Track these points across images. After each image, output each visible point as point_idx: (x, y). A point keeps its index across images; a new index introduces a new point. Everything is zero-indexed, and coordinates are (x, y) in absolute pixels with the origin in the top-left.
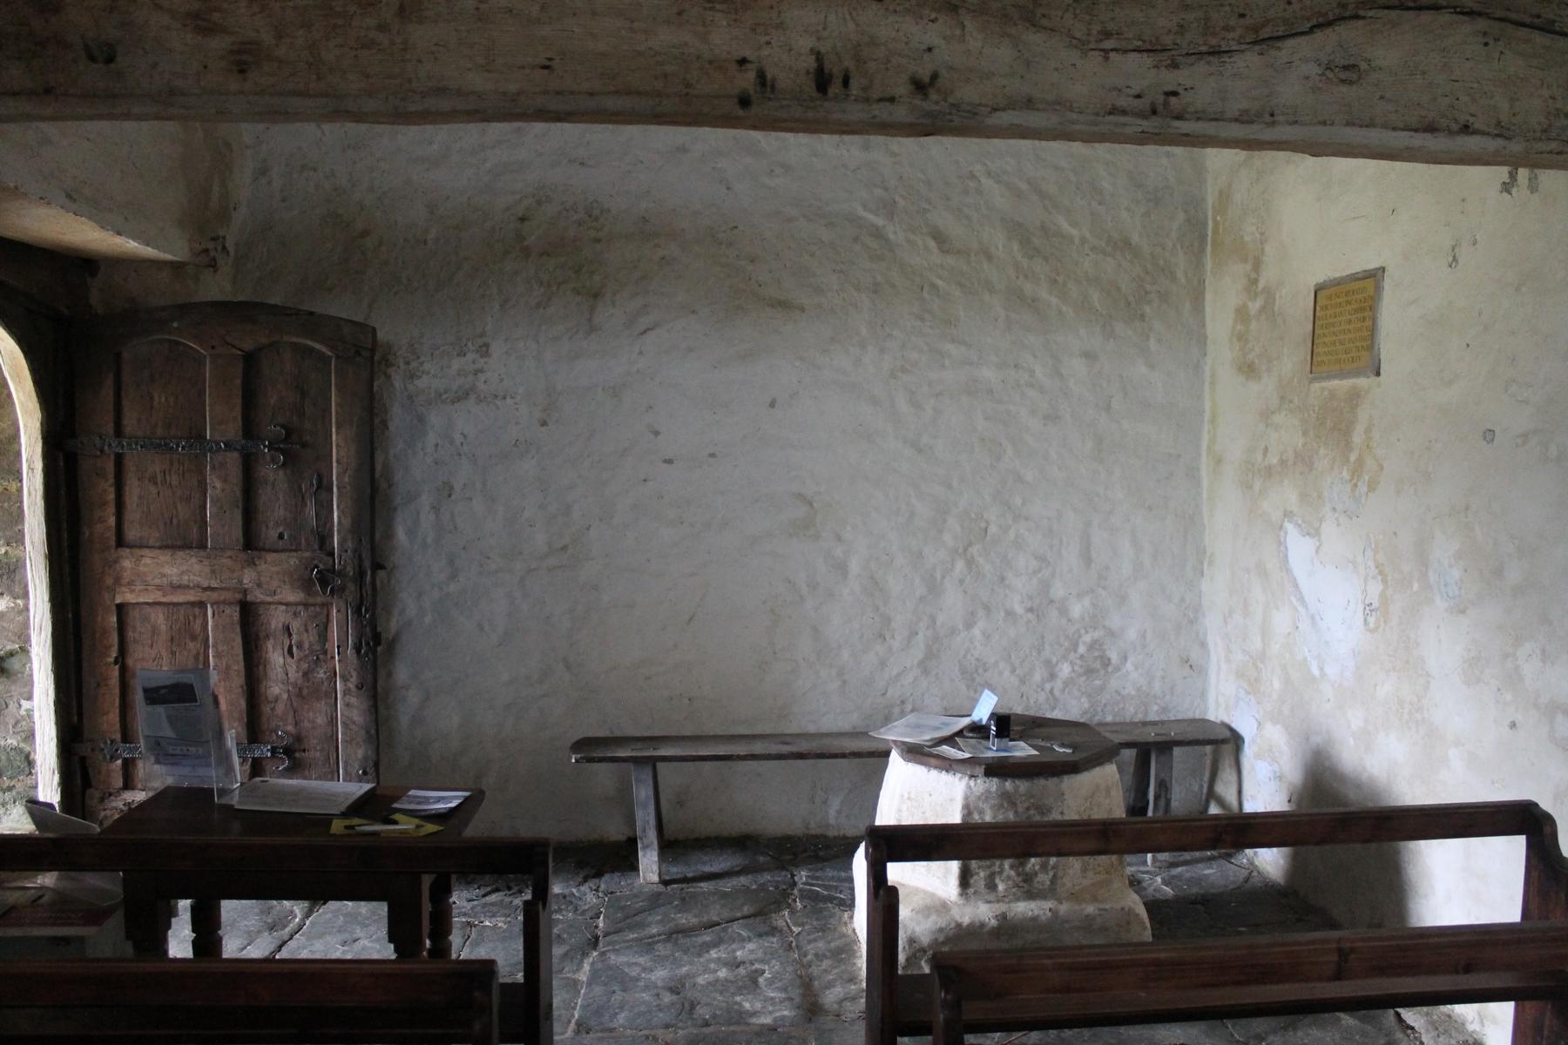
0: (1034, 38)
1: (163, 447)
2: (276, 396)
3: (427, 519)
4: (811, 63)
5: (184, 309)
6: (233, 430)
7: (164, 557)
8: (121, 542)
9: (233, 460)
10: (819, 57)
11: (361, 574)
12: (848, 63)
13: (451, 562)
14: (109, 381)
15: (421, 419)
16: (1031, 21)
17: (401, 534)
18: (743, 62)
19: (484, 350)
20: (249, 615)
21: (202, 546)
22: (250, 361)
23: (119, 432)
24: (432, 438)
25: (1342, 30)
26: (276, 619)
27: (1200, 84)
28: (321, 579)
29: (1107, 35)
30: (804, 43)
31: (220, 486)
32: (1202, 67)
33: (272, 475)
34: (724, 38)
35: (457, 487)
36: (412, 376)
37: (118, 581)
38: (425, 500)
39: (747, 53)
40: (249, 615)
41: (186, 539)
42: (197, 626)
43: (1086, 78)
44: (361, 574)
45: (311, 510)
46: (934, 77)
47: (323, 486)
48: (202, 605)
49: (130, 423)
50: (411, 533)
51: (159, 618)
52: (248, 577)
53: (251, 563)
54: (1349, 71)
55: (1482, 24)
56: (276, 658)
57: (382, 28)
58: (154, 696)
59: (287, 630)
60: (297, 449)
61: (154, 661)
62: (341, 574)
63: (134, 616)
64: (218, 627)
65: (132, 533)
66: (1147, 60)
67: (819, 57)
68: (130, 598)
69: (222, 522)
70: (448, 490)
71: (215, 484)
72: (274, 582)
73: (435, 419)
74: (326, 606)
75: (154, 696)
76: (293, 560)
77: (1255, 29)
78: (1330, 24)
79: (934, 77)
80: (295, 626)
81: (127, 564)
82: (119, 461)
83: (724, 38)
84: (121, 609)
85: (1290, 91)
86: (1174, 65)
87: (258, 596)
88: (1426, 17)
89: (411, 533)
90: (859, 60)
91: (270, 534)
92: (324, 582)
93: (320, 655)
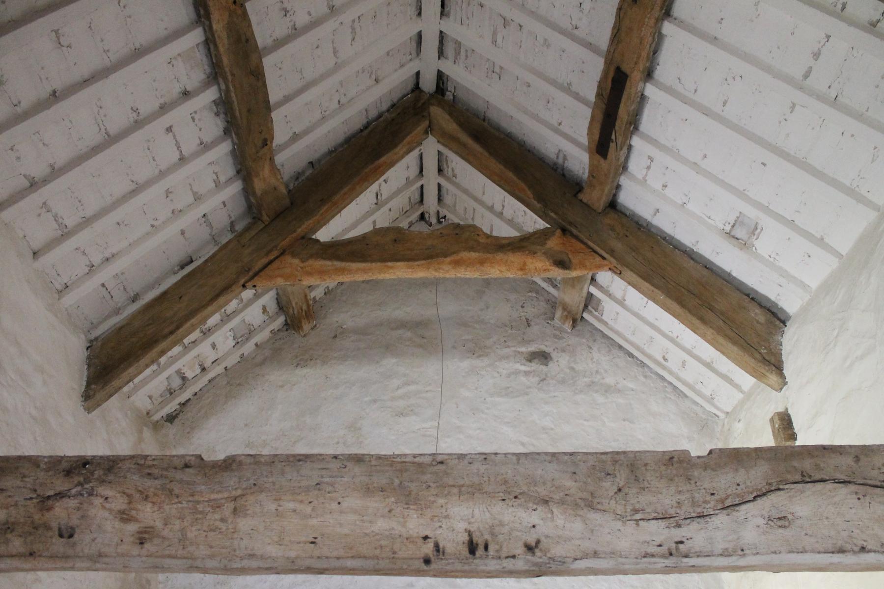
0: (592, 515)
4: (466, 538)
10: (470, 534)
12: (487, 536)
16: (591, 506)
18: (426, 538)
25: (773, 498)
27: (696, 535)
29: (636, 511)
30: (461, 526)
32: (694, 525)
34: (415, 524)
39: (427, 533)
43: (627, 537)
46: (538, 542)
54: (782, 521)
55: (852, 488)
57: (222, 520)
66: (662, 524)
67: (470, 534)
77: (722, 501)
78: (764, 494)
79: (538, 542)
83: (415, 524)
85: (749, 536)
86: (679, 526)
88: (819, 486)
90: (493, 534)
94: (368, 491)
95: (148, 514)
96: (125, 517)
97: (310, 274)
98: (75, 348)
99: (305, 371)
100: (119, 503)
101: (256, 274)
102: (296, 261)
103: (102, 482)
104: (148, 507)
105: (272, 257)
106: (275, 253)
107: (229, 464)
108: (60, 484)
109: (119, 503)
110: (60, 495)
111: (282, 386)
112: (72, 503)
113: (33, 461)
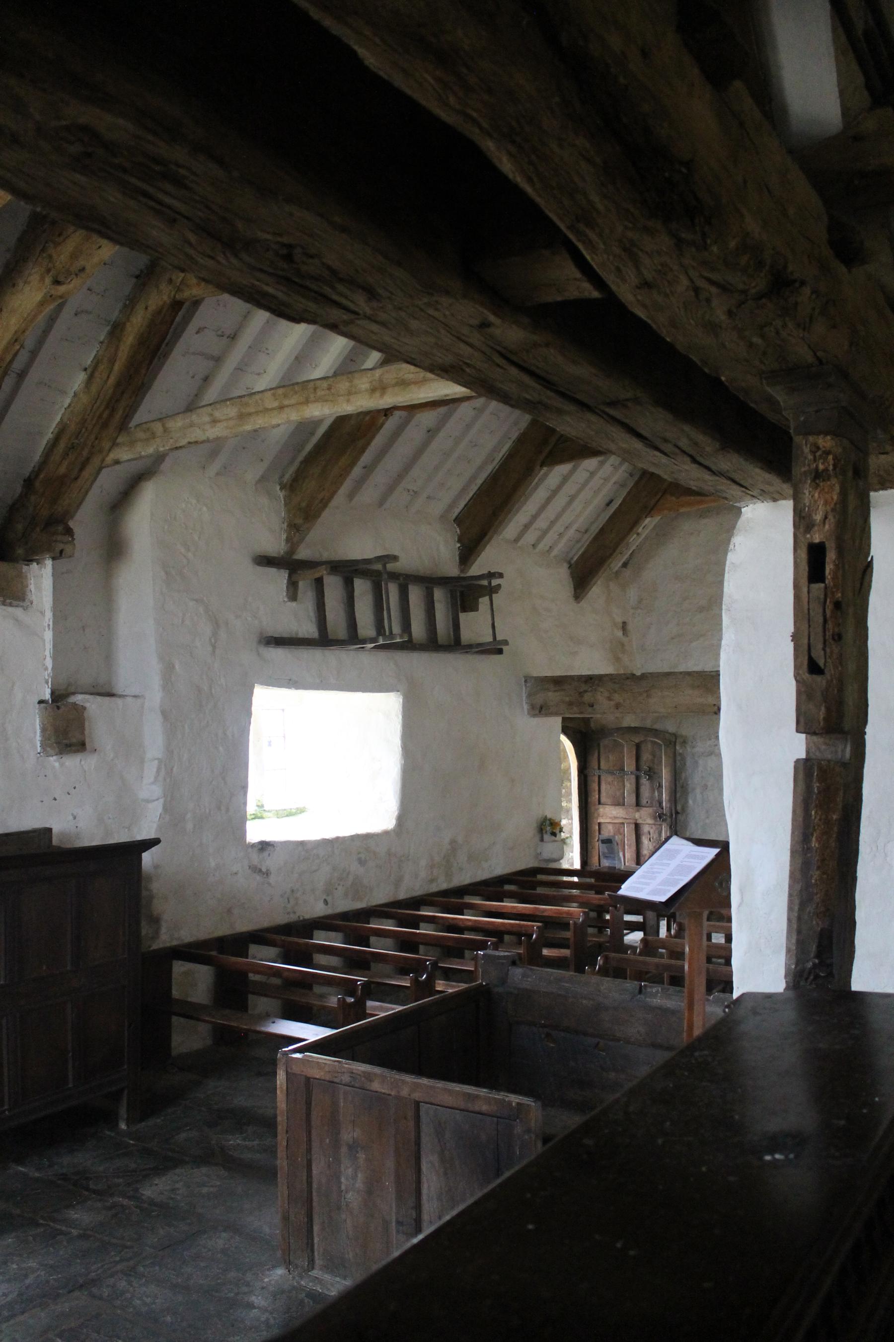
1: (612, 773)
2: (646, 757)
3: (699, 796)
5: (619, 729)
6: (633, 767)
7: (612, 808)
8: (599, 803)
9: (633, 778)
11: (672, 815)
13: (707, 812)
14: (596, 755)
15: (696, 762)
17: (690, 802)
20: (637, 827)
21: (624, 805)
22: (638, 747)
23: (599, 768)
24: (700, 769)
26: (645, 829)
28: (660, 816)
31: (629, 785)
35: (709, 784)
36: (694, 747)
37: (599, 815)
38: (698, 791)
40: (637, 827)
42: (622, 830)
44: (672, 815)
45: (656, 794)
47: (660, 786)
48: (623, 823)
50: (694, 801)
51: (610, 827)
52: (637, 815)
53: (638, 811)
56: (645, 841)
58: (603, 842)
59: (649, 833)
60: (652, 774)
62: (666, 815)
63: (603, 826)
65: (603, 800)
69: (630, 798)
70: (705, 787)
72: (645, 817)
73: (701, 762)
74: (661, 825)
75: (603, 842)
76: (650, 810)
80: (652, 831)
81: (601, 810)
82: (599, 777)
84: (599, 824)
87: (640, 821)
91: (644, 801)
92: (660, 817)
94: (693, 687)
95: (617, 697)
96: (609, 699)
97: (682, 506)
98: (563, 573)
99: (705, 521)
100: (606, 694)
101: (652, 509)
102: (674, 498)
103: (598, 686)
104: (616, 695)
105: (658, 497)
106: (660, 494)
107: (644, 676)
108: (584, 687)
109: (606, 694)
110: (586, 691)
111: (692, 534)
112: (589, 694)
113: (571, 677)
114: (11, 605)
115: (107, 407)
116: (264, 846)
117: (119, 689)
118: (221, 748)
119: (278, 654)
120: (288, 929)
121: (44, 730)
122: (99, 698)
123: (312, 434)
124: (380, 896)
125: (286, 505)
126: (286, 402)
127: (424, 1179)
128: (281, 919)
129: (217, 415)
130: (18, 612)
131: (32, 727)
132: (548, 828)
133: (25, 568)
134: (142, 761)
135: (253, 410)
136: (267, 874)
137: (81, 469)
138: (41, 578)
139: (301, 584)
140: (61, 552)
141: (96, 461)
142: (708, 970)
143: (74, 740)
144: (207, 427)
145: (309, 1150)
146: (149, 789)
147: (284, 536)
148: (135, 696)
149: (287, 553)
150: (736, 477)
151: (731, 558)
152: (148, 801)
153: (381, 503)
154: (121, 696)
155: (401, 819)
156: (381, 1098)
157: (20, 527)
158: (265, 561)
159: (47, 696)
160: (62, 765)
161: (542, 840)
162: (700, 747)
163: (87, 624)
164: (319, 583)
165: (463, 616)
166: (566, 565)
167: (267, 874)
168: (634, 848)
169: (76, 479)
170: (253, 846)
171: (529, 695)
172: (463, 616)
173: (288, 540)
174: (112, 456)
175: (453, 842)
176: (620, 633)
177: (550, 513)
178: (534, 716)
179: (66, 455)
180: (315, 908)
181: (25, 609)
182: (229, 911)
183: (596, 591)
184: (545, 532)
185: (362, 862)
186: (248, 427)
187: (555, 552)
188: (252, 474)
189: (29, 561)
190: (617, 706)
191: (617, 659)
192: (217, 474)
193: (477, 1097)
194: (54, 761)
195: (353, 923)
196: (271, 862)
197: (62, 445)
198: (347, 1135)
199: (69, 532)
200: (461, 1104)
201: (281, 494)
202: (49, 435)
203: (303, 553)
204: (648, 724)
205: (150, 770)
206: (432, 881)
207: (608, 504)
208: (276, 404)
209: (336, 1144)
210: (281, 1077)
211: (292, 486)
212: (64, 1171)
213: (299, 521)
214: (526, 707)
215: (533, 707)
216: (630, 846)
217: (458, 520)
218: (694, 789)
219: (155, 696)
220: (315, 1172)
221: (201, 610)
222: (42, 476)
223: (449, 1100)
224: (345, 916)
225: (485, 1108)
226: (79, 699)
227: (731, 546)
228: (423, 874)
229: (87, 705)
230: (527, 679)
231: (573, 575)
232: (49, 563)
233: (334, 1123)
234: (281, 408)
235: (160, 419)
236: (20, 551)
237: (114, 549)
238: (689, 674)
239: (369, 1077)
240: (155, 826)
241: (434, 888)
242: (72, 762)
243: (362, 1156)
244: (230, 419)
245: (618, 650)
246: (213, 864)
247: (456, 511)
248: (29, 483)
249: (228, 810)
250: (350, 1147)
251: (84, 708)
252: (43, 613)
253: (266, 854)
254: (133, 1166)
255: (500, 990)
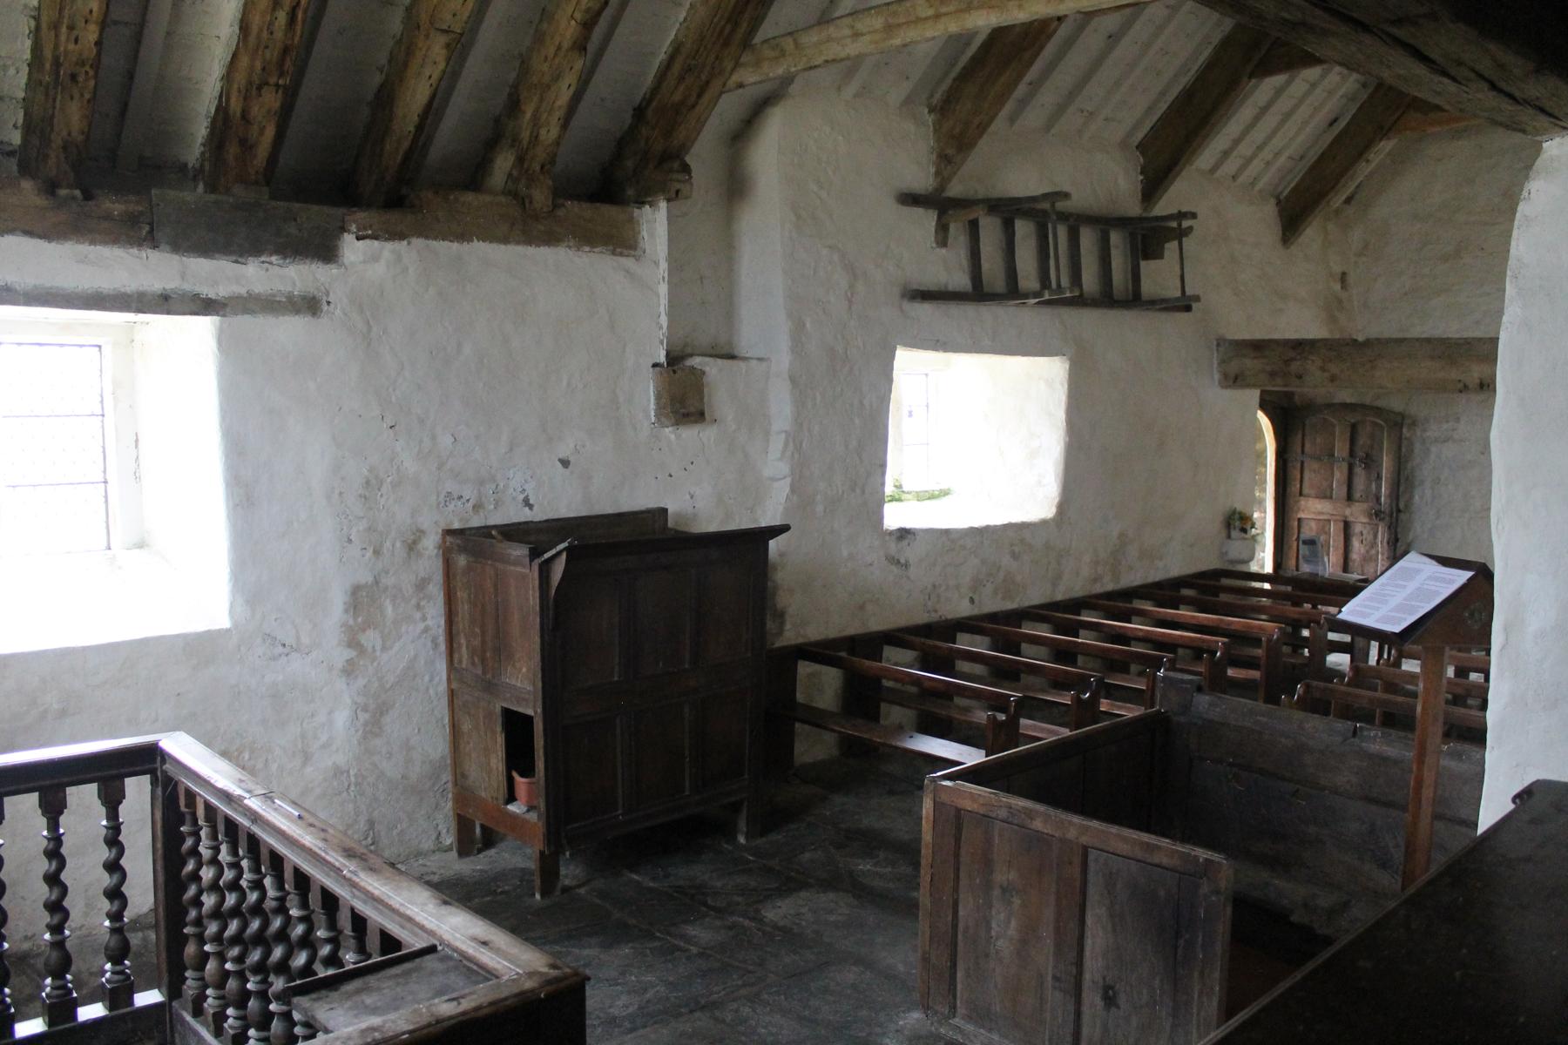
1: (1319, 459)
2: (1362, 440)
3: (1428, 492)
5: (1330, 406)
6: (1345, 454)
8: (1301, 494)
9: (1345, 466)
19: (1458, 420)
20: (1347, 526)
22: (1354, 427)
24: (1433, 457)
26: (1357, 528)
28: (1377, 514)
30: (1476, 375)
31: (1339, 475)
33: (1359, 471)
34: (1454, 374)
40: (1347, 526)
41: (1325, 495)
47: (1379, 477)
49: (1307, 446)
50: (1421, 498)
51: (1313, 524)
52: (1348, 512)
56: (1356, 543)
58: (1305, 542)
60: (1370, 462)
61: (1309, 531)
63: (1304, 524)
64: (1335, 530)
65: (1306, 491)
68: (1301, 515)
69: (1339, 489)
70: (1437, 481)
71: (1337, 474)
72: (1358, 514)
73: (1433, 449)
75: (1305, 542)
76: (1365, 506)
83: (1454, 374)
87: (1351, 519)
89: (1421, 498)
91: (1357, 495)
92: (1377, 515)
93: (1373, 545)
94: (1432, 358)
95: (1334, 368)
96: (1323, 369)
98: (1270, 210)
107: (1368, 343)
108: (1292, 354)
109: (1319, 363)
110: (1292, 359)
113: (1276, 342)
114: (621, 254)
115: (729, 20)
116: (903, 534)
117: (743, 352)
118: (857, 421)
119: (925, 310)
120: (927, 630)
121: (658, 397)
122: (719, 361)
123: (968, 44)
124: (1035, 596)
125: (935, 131)
126: (944, 10)
127: (1088, 934)
128: (921, 618)
129: (859, 26)
130: (628, 262)
131: (646, 394)
132: (1237, 523)
133: (636, 212)
134: (767, 433)
135: (902, 20)
136: (906, 566)
137: (699, 96)
138: (655, 224)
139: (952, 228)
140: (677, 192)
141: (716, 85)
142: (1446, 714)
143: (692, 409)
144: (849, 41)
145: (956, 889)
146: (775, 465)
147: (933, 170)
148: (759, 359)
149: (936, 190)
150: (1547, 105)
151: (1523, 209)
152: (773, 479)
153: (1048, 127)
154: (745, 359)
155: (1062, 507)
156: (1040, 839)
157: (630, 164)
158: (911, 199)
159: (662, 359)
160: (678, 437)
161: (1229, 537)
162: (1433, 431)
163: (706, 275)
164: (974, 226)
165: (1143, 264)
166: (1273, 201)
167: (906, 566)
168: (1341, 551)
169: (694, 106)
170: (891, 533)
171: (1222, 362)
172: (1143, 264)
173: (937, 173)
174: (735, 78)
175: (1122, 535)
176: (1337, 287)
177: (1258, 135)
178: (1227, 387)
179: (681, 79)
180: (960, 607)
181: (637, 259)
182: (862, 607)
183: (1311, 234)
184: (1249, 161)
185: (1015, 556)
186: (897, 42)
187: (1260, 185)
188: (896, 95)
189: (641, 203)
190: (1333, 379)
191: (1332, 320)
192: (855, 96)
193: (1159, 848)
194: (669, 432)
195: (1002, 627)
196: (911, 553)
197: (677, 68)
198: (1002, 876)
199: (686, 169)
200: (1139, 854)
201: (930, 119)
202: (662, 56)
203: (955, 190)
204: (1368, 400)
205: (777, 444)
206: (1095, 580)
207: (1331, 124)
208: (931, 12)
209: (988, 886)
210: (927, 806)
211: (943, 109)
212: (681, 883)
213: (950, 151)
214: (1217, 376)
215: (1225, 376)
216: (1336, 549)
217: (1142, 147)
218: (1422, 482)
219: (782, 360)
220: (961, 913)
221: (836, 257)
222: (654, 104)
223: (1123, 848)
224: (993, 617)
225: (1165, 861)
226: (696, 361)
227: (1525, 193)
228: (1086, 572)
229: (707, 369)
230: (1221, 342)
231: (1281, 213)
232: (663, 205)
233: (987, 863)
234: (937, 16)
235: (790, 34)
236: (630, 192)
237: (735, 187)
238: (1428, 340)
239: (1030, 814)
240: (781, 508)
241: (1098, 589)
242: (690, 433)
243: (1017, 901)
244: (875, 31)
245: (1333, 307)
246: (845, 553)
247: (1140, 135)
248: (639, 112)
249: (863, 492)
250: (1004, 890)
251: (704, 373)
252: (656, 263)
253: (905, 542)
254: (753, 884)
255: (1182, 719)
